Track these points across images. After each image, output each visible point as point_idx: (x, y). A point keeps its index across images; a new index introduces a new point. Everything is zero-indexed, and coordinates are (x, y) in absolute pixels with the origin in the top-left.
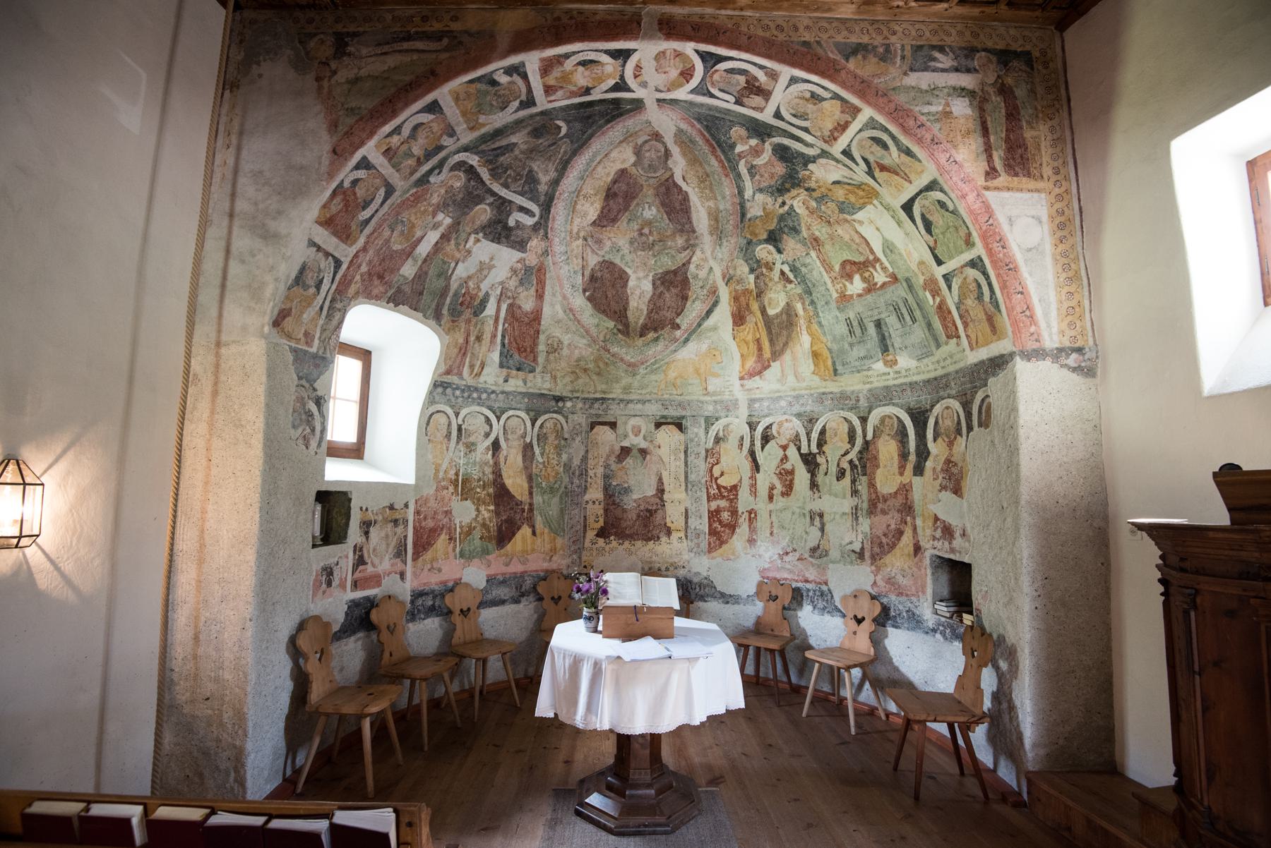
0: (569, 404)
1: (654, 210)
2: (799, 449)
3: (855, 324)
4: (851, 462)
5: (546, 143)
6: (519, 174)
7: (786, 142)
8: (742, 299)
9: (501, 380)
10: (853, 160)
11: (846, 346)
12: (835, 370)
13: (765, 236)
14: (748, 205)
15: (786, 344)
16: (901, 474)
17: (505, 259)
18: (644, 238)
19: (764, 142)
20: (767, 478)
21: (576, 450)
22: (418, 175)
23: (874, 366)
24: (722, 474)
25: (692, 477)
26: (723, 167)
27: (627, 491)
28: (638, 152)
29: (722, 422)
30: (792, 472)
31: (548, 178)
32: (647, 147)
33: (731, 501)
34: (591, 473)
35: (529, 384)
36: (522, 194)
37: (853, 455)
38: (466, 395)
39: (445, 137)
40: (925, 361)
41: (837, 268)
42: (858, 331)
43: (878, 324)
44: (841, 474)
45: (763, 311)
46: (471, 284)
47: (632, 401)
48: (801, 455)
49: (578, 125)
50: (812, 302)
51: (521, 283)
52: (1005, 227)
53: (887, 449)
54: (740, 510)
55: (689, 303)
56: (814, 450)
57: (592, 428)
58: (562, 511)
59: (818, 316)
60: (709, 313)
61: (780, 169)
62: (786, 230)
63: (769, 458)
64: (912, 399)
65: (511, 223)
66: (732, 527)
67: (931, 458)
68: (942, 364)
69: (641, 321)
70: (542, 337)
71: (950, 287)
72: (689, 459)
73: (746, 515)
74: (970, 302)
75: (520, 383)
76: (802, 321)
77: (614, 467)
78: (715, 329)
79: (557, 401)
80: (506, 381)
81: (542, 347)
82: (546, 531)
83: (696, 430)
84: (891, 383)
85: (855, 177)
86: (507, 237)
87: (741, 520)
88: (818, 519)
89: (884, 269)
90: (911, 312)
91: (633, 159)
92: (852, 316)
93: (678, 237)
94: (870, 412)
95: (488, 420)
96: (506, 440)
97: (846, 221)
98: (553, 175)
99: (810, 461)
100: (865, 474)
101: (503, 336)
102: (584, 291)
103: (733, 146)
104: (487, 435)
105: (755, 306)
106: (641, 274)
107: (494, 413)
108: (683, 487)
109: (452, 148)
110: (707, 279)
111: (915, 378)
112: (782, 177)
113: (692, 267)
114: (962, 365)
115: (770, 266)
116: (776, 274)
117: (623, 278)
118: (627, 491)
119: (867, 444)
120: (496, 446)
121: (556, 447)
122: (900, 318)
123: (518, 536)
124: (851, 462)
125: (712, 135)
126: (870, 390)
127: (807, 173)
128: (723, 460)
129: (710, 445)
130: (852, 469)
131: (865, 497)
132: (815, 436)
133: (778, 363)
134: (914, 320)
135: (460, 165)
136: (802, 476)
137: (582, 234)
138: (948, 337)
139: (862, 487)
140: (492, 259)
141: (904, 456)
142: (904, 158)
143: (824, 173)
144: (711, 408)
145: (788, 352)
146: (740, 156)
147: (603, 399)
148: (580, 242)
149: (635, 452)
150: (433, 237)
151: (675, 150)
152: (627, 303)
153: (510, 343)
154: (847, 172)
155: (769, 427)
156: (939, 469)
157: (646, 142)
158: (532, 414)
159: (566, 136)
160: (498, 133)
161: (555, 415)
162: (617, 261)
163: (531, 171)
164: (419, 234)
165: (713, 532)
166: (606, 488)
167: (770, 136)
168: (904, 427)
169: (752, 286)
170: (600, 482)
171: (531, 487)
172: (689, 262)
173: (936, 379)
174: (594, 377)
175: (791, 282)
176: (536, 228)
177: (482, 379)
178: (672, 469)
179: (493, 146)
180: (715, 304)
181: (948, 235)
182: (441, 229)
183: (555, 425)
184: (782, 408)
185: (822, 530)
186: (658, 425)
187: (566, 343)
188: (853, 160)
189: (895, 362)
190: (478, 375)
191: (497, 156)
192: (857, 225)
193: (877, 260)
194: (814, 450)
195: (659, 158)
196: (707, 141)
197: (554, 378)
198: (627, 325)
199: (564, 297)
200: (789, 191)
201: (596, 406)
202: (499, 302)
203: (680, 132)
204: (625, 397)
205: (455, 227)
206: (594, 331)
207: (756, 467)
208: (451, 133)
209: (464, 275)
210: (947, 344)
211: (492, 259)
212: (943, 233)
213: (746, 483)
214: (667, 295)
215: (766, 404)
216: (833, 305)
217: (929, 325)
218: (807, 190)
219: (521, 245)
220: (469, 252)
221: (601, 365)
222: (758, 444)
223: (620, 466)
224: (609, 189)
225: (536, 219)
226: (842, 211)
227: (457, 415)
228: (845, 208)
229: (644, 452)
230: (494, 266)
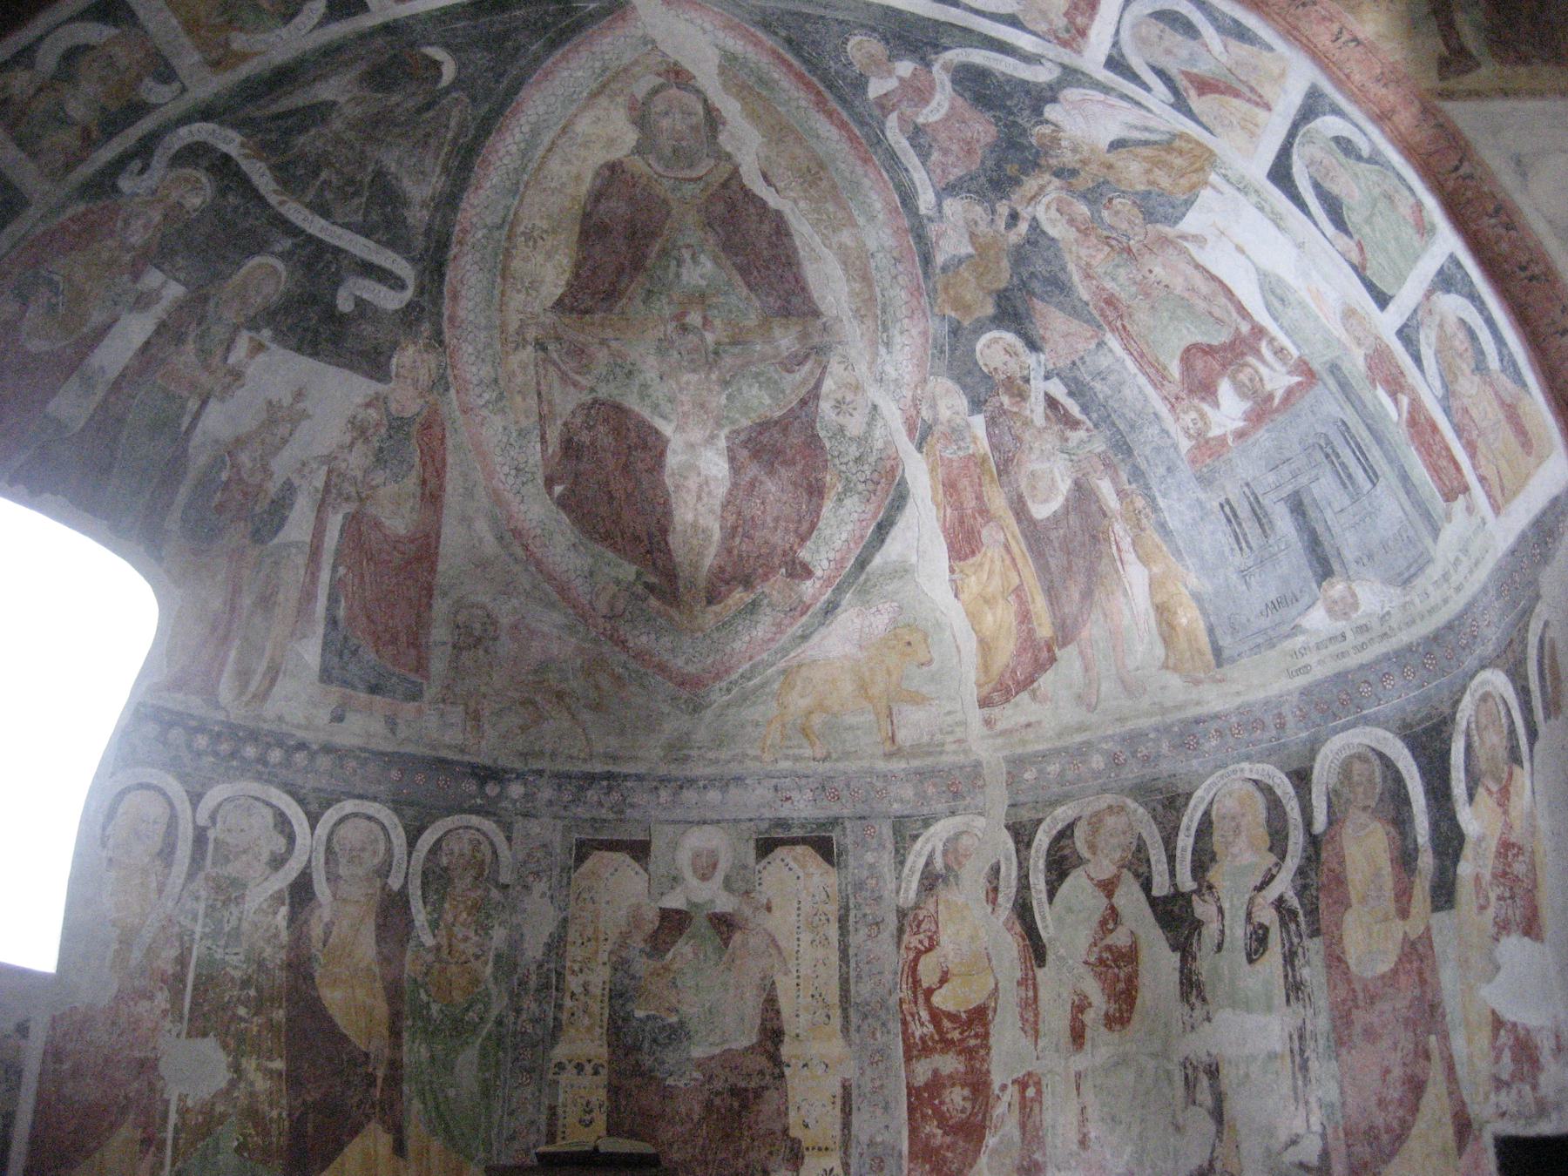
0: (516, 790)
1: (707, 265)
2: (1147, 886)
3: (1244, 511)
4: (1280, 903)
5: (410, 104)
6: (351, 181)
7: (979, 57)
8: (964, 483)
9: (323, 716)
10: (1134, 77)
12: (1217, 651)
13: (990, 310)
14: (932, 230)
15: (1087, 595)
16: (1404, 914)
17: (336, 396)
18: (692, 338)
19: (928, 65)
20: (1069, 975)
21: (537, 920)
22: (85, 171)
24: (943, 980)
25: (862, 990)
26: (852, 138)
27: (677, 1034)
28: (641, 117)
29: (941, 830)
30: (1129, 956)
31: (427, 192)
32: (659, 105)
33: (970, 1054)
34: (574, 983)
35: (403, 731)
36: (366, 231)
37: (1283, 885)
38: (224, 747)
39: (148, 82)
40: (1419, 582)
41: (1175, 369)
43: (1297, 506)
44: (1258, 941)
45: (1019, 508)
46: (244, 458)
47: (692, 782)
48: (1153, 902)
49: (481, 58)
50: (1137, 474)
51: (380, 458)
52: (1507, 180)
53: (1365, 850)
54: (997, 1079)
55: (828, 505)
56: (1187, 883)
57: (580, 859)
58: (486, 1092)
59: (1156, 509)
60: (883, 529)
61: (982, 129)
62: (1036, 286)
63: (1069, 921)
65: (344, 304)
66: (972, 1131)
67: (1468, 851)
68: (1455, 579)
69: (709, 560)
70: (440, 607)
71: (1417, 359)
72: (854, 940)
73: (1012, 1093)
74: (1468, 385)
75: (378, 726)
76: (1119, 529)
77: (642, 966)
78: (902, 571)
79: (483, 782)
80: (338, 718)
81: (440, 633)
82: (436, 1144)
83: (870, 856)
84: (1353, 661)
85: (1152, 124)
86: (337, 340)
87: (999, 1110)
88: (1204, 1082)
89: (1280, 352)
90: (1360, 453)
91: (631, 137)
92: (1234, 492)
93: (777, 332)
94: (1313, 753)
95: (283, 823)
96: (333, 878)
97: (1165, 241)
98: (436, 183)
99: (1175, 916)
100: (1315, 933)
101: (333, 600)
102: (550, 482)
103: (860, 84)
104: (277, 862)
105: (998, 501)
106: (697, 435)
107: (301, 802)
108: (837, 1021)
109: (173, 110)
110: (864, 440)
112: (992, 148)
113: (825, 406)
115: (1017, 388)
116: (1036, 409)
117: (650, 446)
118: (677, 1034)
119: (1314, 842)
120: (301, 892)
121: (476, 908)
122: (1345, 479)
123: (353, 1152)
124: (1280, 903)
125: (806, 61)
126: (1305, 692)
127: (1046, 130)
128: (944, 939)
129: (910, 891)
130: (1284, 924)
131: (1322, 1002)
132: (1185, 842)
133: (1072, 649)
134: (1373, 477)
135: (194, 154)
136: (1159, 963)
137: (532, 333)
139: (1312, 972)
140: (299, 395)
141: (1405, 859)
142: (1241, 50)
143: (1086, 123)
144: (908, 792)
145: (1096, 614)
146: (884, 104)
147: (610, 776)
148: (528, 354)
149: (700, 922)
150: (136, 329)
151: (730, 107)
152: (668, 514)
153: (351, 619)
154: (1132, 115)
155: (1066, 833)
156: (1487, 876)
157: (655, 91)
158: (410, 812)
159: (456, 84)
160: (284, 77)
161: (475, 820)
162: (632, 402)
163: (380, 174)
164: (97, 317)
165: (922, 1151)
166: (618, 1028)
167: (938, 48)
168: (1399, 780)
169: (984, 446)
170: (599, 1009)
171: (396, 1017)
172: (815, 394)
173: (1449, 627)
174: (586, 716)
175: (1074, 424)
176: (410, 317)
177: (270, 709)
178: (805, 974)
179: (275, 108)
180: (900, 499)
181: (1378, 220)
182: (158, 311)
183: (476, 846)
184: (1097, 775)
185: (1218, 1114)
186: (766, 847)
187: (505, 621)
188: (1134, 77)
190: (263, 696)
191: (288, 132)
192: (1192, 248)
193: (1259, 332)
194: (1187, 883)
195: (694, 128)
196: (800, 77)
197: (476, 717)
198: (671, 575)
199: (497, 498)
200: (1016, 182)
201: (592, 795)
202: (321, 507)
203: (729, 62)
204: (675, 770)
205: (196, 305)
206: (580, 588)
207: (1036, 951)
208: (166, 74)
209: (227, 433)
211: (299, 395)
212: (1368, 221)
213: (1010, 998)
214: (771, 486)
215: (1053, 768)
216: (1185, 471)
218: (1058, 173)
219: (374, 363)
220: (237, 375)
221: (605, 682)
222: (1038, 882)
223: (654, 964)
224: (587, 216)
225: (408, 294)
226: (1149, 216)
227: (195, 799)
228: (1159, 209)
229: (724, 925)
230: (304, 415)
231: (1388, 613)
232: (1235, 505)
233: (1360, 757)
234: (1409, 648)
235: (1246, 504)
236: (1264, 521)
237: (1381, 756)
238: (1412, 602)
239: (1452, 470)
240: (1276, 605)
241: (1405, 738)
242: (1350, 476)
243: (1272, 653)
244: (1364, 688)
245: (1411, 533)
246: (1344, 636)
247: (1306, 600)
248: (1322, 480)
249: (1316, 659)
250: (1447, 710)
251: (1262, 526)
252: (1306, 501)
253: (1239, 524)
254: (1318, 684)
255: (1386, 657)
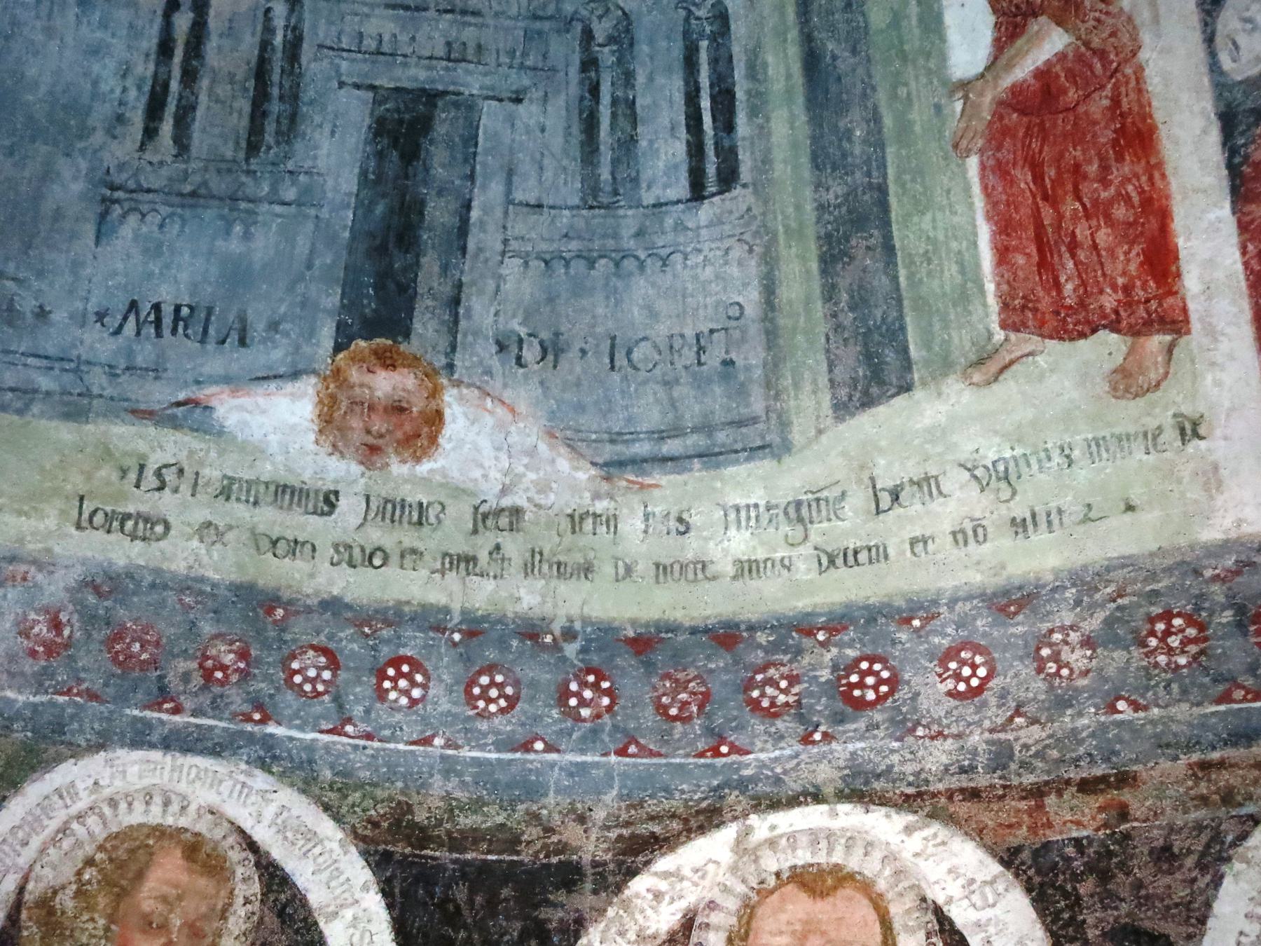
11: (70, 186)
23: (232, 410)
40: (668, 489)
42: (219, 118)
43: (405, 128)
64: (442, 748)
68: (851, 525)
111: (527, 597)
114: (1122, 539)
126: (106, 585)
134: (712, 171)
138: (1017, 314)
173: (726, 636)
189: (419, 430)
210: (987, 365)
217: (857, 227)
231: (517, 512)
232: (213, 23)
233: (195, 850)
234: (531, 631)
235: (249, 44)
236: (275, 107)
237: (274, 877)
238: (611, 521)
239: (1126, 263)
240: (186, 320)
241: (379, 861)
242: (628, 144)
243: (65, 433)
244: (310, 665)
245: (752, 357)
246: (330, 501)
247: (277, 355)
248: (528, 112)
249: (200, 515)
250: (591, 847)
251: (258, 114)
252: (444, 124)
253: (190, 76)
254: (161, 583)
255: (432, 620)
